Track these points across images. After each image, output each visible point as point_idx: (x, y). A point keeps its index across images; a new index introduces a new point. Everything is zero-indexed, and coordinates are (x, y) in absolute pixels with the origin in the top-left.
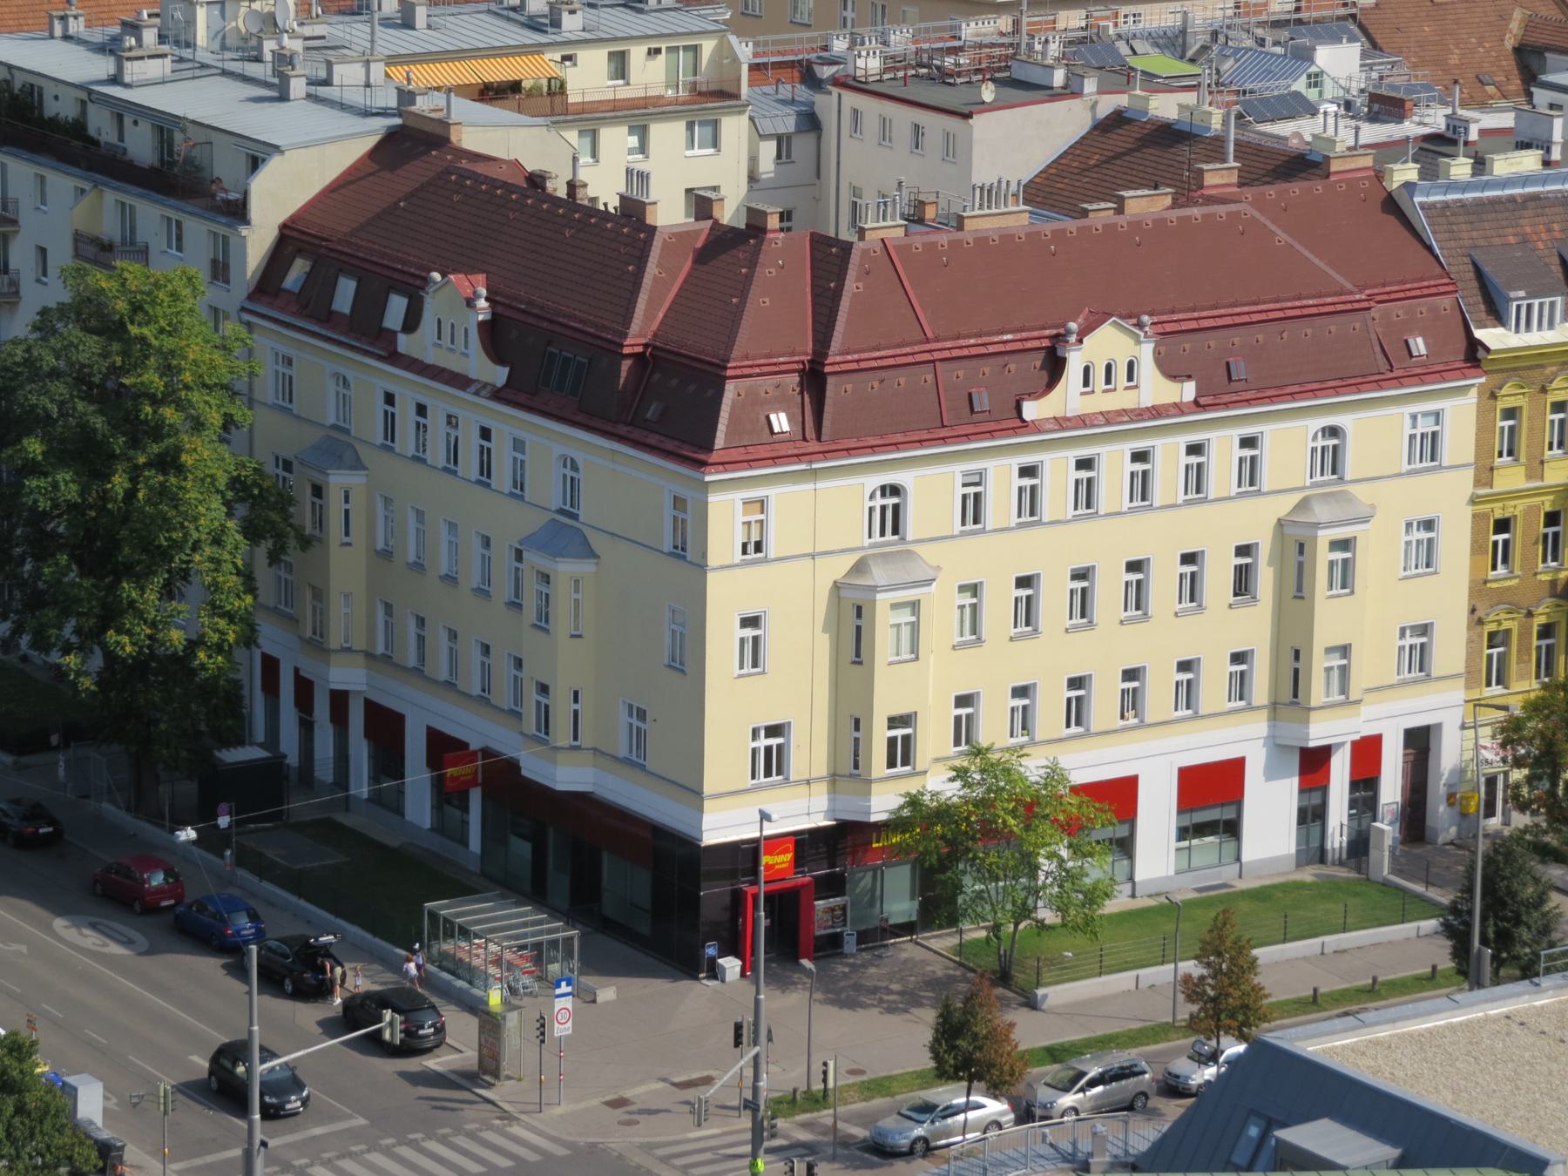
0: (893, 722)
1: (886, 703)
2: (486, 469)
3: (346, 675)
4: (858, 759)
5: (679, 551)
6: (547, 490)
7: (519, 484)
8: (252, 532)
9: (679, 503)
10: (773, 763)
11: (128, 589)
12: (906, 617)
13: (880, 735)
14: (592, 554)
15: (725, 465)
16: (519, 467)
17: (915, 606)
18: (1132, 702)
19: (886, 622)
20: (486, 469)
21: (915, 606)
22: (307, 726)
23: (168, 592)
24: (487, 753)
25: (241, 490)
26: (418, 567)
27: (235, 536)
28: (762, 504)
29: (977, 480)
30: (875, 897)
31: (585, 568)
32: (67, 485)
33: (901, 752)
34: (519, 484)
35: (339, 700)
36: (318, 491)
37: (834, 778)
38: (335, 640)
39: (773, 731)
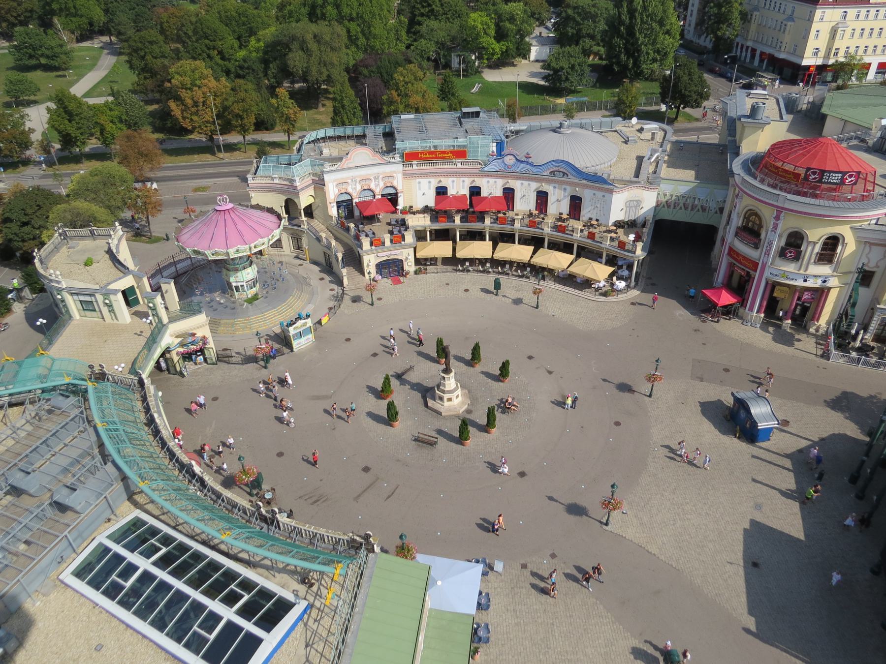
0: (836, 49)
1: (835, 47)
2: (779, 9)
3: (750, 44)
4: (829, 54)
5: (809, 20)
6: (789, 12)
7: (784, 11)
8: (741, 19)
9: (811, 12)
10: (816, 54)
11: (722, 25)
12: (842, 32)
13: (833, 51)
14: (794, 21)
15: (820, 5)
16: (785, 9)
17: (844, 31)
18: (874, 51)
19: (839, 32)
20: (779, 9)
21: (844, 31)
22: (741, 52)
23: (727, 26)
24: (769, 54)
25: (741, 13)
26: (765, 26)
27: (739, 19)
28: (824, 12)
29: (860, 12)
30: (826, 77)
31: (793, 23)
32: (716, 10)
33: (836, 54)
34: (784, 11)
35: (747, 47)
36: (751, 15)
37: (824, 57)
38: (749, 38)
39: (817, 49)
